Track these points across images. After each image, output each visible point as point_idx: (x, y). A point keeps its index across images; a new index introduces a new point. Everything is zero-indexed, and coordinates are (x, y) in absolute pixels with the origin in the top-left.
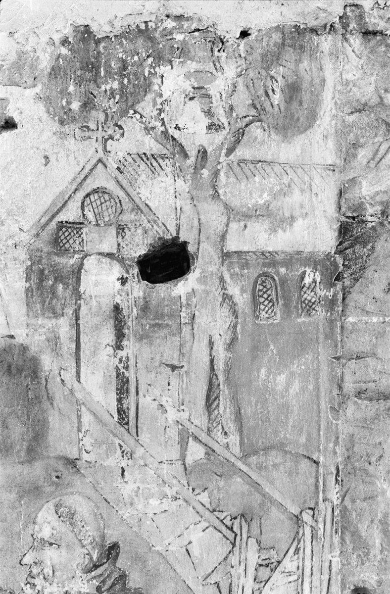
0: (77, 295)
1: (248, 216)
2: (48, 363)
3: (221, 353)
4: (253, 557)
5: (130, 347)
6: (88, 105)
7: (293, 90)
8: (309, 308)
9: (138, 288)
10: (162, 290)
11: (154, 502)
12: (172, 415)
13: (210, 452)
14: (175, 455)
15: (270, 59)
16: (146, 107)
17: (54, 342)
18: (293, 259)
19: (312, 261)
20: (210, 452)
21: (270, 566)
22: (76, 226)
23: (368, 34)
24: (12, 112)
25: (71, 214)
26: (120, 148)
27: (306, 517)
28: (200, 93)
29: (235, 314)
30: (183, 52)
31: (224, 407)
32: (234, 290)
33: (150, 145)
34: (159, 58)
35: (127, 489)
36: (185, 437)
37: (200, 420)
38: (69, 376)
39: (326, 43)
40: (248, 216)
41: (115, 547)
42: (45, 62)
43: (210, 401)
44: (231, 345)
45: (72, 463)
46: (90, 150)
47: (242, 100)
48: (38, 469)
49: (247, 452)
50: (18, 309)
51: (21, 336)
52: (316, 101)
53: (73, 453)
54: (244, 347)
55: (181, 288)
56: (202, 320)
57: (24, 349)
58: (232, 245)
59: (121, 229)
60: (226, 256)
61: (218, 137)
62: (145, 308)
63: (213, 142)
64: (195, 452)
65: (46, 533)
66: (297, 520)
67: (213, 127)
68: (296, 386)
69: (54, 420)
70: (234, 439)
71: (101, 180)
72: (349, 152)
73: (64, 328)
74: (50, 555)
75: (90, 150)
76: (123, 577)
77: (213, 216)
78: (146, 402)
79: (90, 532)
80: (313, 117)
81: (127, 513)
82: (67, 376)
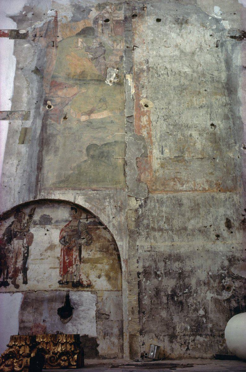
0: (98, 23)
1: (115, 17)
2: (95, 28)
3: (112, 27)
4: (116, 44)
5: (103, 27)
6: (99, 9)
7: (120, 8)
8: (122, 24)
9: (104, 23)
10: (106, 23)
11: (106, 39)
12: (107, 32)
13: (111, 35)
14: (108, 35)
15: (117, 5)
16: (105, 9)
17: (96, 27)
18: (120, 20)
19: (122, 20)
20: (111, 35)
21: (118, 44)
22: (98, 18)
23: (127, 3)
24: (92, 9)
25: (98, 17)
26: (102, 12)
27: (121, 40)
28: (111, 8)
29: (114, 24)
30: (109, 5)
31: (113, 32)
32: (114, 23)
33: (105, 12)
34: (106, 5)
35: (103, 38)
36: (109, 34)
37: (110, 33)
38: (97, 29)
39: (123, 4)
40: (115, 17)
41: (101, 43)
42: (95, 6)
43: (111, 31)
44: (114, 27)
45: (97, 36)
46: (100, 12)
47: (115, 9)
48: (94, 37)
49: (115, 35)
50: (92, 24)
51: (92, 26)
52: (122, 8)
53: (97, 35)
54: (115, 27)
55: (108, 23)
56: (111, 25)
57: (93, 27)
58: (114, 19)
59: (102, 18)
60: (113, 20)
61: (112, 11)
62: (105, 24)
63: (112, 12)
64: (110, 35)
65: (94, 42)
66: (121, 41)
67: (112, 10)
68: (120, 30)
69: (95, 33)
70: (114, 34)
71: (100, 14)
72: (125, 11)
73: (97, 26)
74: (95, 44)
75: (100, 12)
76: (102, 45)
77: (112, 17)
78: (105, 31)
79: (99, 42)
80: (122, 9)
81: (103, 40)
82: (97, 29)
